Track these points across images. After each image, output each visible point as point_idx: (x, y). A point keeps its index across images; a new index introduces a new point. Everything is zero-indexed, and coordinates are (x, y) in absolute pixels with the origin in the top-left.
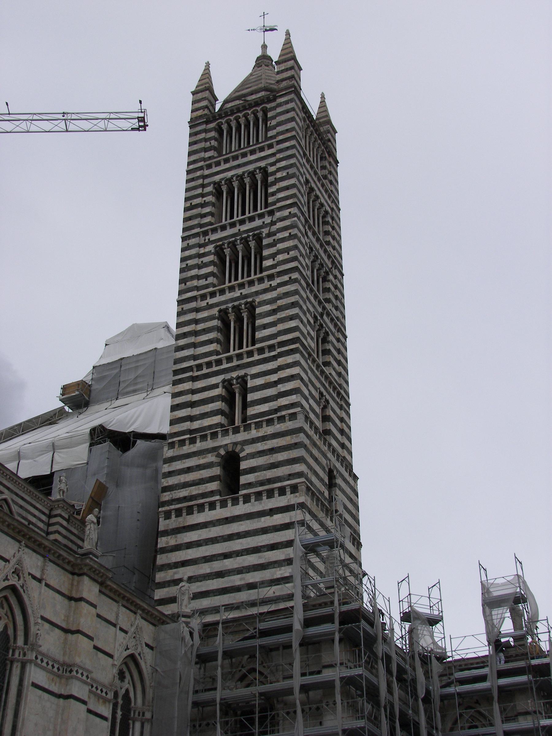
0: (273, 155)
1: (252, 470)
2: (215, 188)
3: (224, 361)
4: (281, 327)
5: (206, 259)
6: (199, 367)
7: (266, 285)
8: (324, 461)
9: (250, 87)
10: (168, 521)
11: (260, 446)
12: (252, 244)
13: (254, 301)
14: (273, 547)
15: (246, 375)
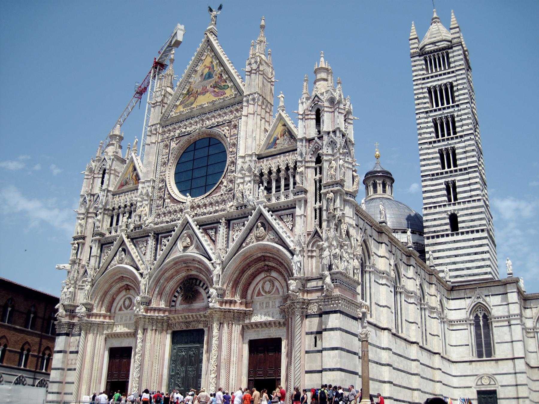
0: (455, 76)
1: (463, 222)
2: (428, 90)
3: (444, 173)
4: (469, 160)
5: (429, 125)
6: (433, 175)
7: (459, 140)
8: (487, 216)
9: (435, 37)
10: (428, 240)
11: (466, 212)
12: (450, 119)
13: (454, 147)
14: (476, 254)
15: (455, 180)
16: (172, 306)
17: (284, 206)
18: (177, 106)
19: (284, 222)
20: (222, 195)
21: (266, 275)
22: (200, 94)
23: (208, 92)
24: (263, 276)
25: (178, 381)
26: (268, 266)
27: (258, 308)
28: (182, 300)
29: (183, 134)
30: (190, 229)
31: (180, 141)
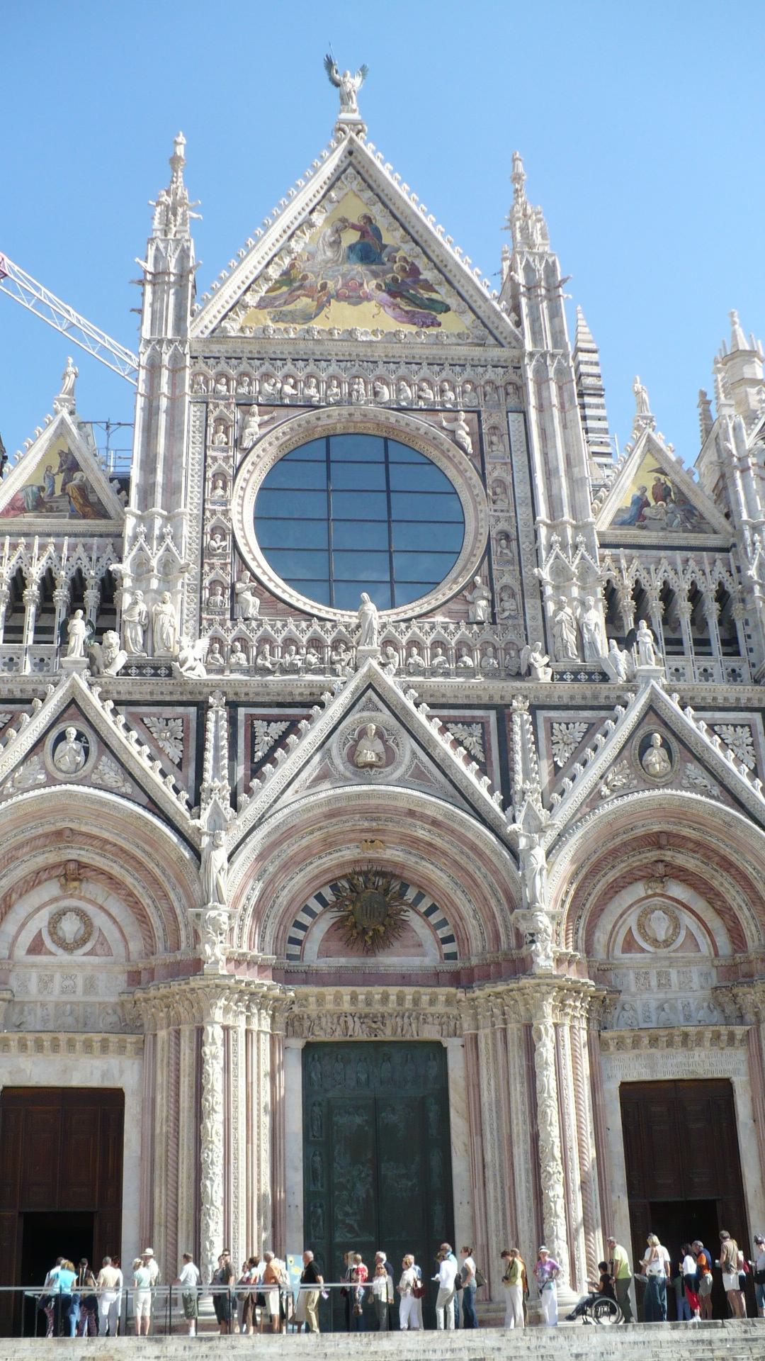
16: (290, 957)
17: (726, 699)
18: (245, 307)
19: (727, 745)
20: (480, 623)
21: (650, 892)
22: (339, 297)
23: (368, 298)
24: (643, 895)
25: (347, 1214)
26: (667, 865)
27: (633, 989)
28: (327, 938)
29: (287, 401)
30: (378, 709)
31: (272, 418)
